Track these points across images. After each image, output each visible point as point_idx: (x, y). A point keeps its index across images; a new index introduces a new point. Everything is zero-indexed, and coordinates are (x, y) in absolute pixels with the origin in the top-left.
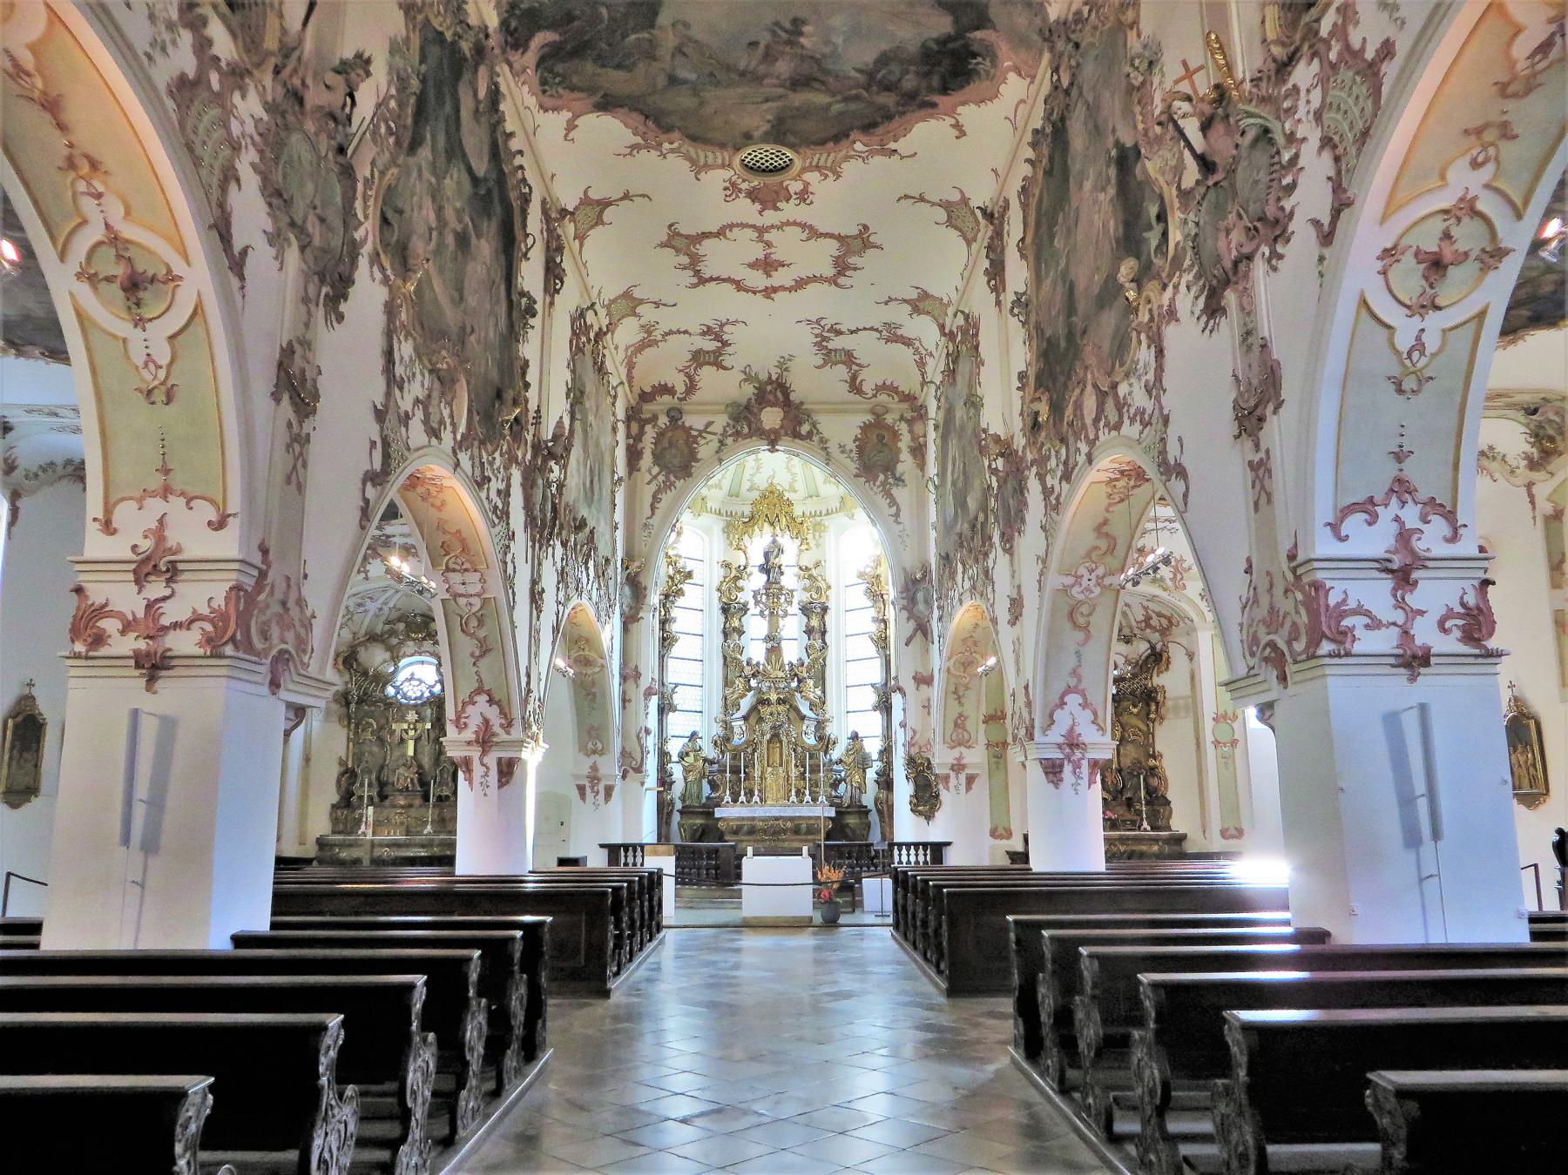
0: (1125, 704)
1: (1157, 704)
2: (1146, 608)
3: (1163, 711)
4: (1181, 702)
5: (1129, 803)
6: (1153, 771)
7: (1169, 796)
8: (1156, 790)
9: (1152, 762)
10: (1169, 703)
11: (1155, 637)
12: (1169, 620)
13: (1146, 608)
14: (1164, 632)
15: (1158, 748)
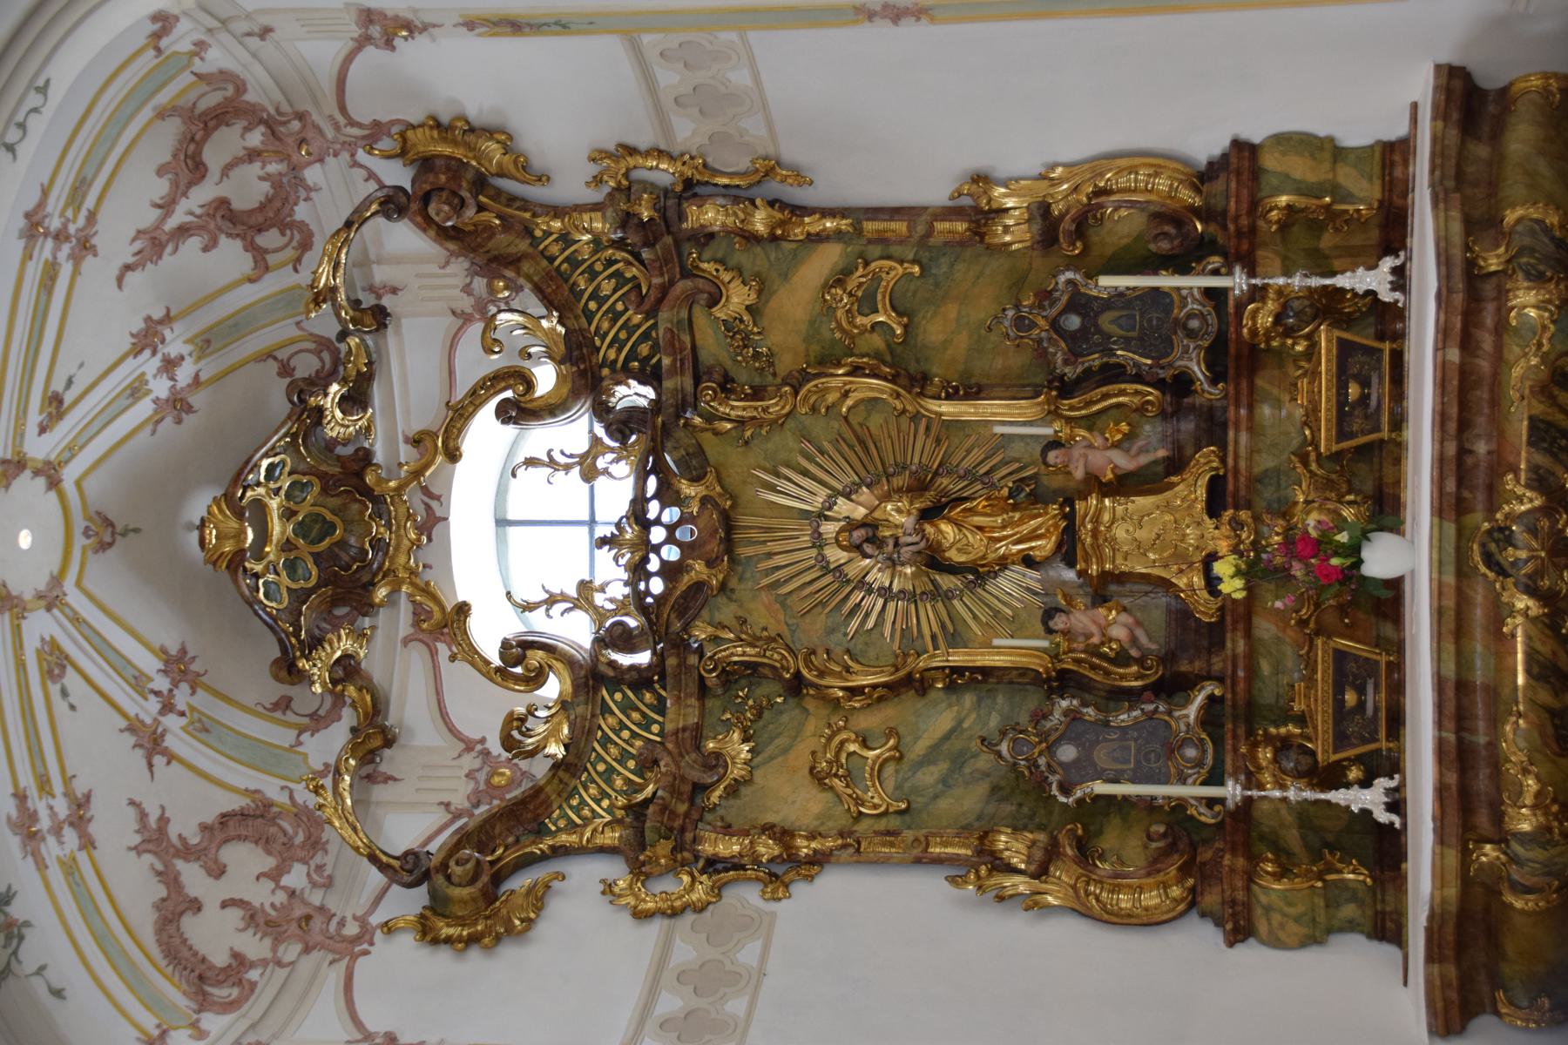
0: (712, 345)
1: (690, 189)
2: (154, 244)
3: (733, 162)
4: (669, 78)
5: (1238, 359)
6: (1066, 229)
7: (1206, 146)
8: (1168, 218)
9: (1014, 233)
10: (687, 132)
11: (332, 190)
12: (202, 124)
13: (154, 244)
14: (287, 132)
15: (934, 191)
